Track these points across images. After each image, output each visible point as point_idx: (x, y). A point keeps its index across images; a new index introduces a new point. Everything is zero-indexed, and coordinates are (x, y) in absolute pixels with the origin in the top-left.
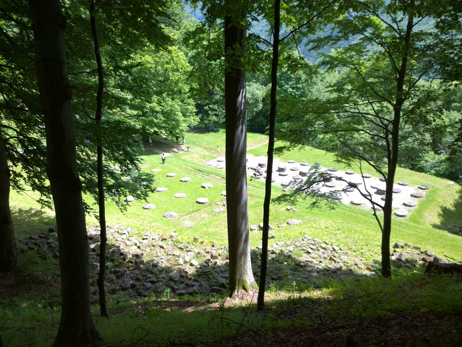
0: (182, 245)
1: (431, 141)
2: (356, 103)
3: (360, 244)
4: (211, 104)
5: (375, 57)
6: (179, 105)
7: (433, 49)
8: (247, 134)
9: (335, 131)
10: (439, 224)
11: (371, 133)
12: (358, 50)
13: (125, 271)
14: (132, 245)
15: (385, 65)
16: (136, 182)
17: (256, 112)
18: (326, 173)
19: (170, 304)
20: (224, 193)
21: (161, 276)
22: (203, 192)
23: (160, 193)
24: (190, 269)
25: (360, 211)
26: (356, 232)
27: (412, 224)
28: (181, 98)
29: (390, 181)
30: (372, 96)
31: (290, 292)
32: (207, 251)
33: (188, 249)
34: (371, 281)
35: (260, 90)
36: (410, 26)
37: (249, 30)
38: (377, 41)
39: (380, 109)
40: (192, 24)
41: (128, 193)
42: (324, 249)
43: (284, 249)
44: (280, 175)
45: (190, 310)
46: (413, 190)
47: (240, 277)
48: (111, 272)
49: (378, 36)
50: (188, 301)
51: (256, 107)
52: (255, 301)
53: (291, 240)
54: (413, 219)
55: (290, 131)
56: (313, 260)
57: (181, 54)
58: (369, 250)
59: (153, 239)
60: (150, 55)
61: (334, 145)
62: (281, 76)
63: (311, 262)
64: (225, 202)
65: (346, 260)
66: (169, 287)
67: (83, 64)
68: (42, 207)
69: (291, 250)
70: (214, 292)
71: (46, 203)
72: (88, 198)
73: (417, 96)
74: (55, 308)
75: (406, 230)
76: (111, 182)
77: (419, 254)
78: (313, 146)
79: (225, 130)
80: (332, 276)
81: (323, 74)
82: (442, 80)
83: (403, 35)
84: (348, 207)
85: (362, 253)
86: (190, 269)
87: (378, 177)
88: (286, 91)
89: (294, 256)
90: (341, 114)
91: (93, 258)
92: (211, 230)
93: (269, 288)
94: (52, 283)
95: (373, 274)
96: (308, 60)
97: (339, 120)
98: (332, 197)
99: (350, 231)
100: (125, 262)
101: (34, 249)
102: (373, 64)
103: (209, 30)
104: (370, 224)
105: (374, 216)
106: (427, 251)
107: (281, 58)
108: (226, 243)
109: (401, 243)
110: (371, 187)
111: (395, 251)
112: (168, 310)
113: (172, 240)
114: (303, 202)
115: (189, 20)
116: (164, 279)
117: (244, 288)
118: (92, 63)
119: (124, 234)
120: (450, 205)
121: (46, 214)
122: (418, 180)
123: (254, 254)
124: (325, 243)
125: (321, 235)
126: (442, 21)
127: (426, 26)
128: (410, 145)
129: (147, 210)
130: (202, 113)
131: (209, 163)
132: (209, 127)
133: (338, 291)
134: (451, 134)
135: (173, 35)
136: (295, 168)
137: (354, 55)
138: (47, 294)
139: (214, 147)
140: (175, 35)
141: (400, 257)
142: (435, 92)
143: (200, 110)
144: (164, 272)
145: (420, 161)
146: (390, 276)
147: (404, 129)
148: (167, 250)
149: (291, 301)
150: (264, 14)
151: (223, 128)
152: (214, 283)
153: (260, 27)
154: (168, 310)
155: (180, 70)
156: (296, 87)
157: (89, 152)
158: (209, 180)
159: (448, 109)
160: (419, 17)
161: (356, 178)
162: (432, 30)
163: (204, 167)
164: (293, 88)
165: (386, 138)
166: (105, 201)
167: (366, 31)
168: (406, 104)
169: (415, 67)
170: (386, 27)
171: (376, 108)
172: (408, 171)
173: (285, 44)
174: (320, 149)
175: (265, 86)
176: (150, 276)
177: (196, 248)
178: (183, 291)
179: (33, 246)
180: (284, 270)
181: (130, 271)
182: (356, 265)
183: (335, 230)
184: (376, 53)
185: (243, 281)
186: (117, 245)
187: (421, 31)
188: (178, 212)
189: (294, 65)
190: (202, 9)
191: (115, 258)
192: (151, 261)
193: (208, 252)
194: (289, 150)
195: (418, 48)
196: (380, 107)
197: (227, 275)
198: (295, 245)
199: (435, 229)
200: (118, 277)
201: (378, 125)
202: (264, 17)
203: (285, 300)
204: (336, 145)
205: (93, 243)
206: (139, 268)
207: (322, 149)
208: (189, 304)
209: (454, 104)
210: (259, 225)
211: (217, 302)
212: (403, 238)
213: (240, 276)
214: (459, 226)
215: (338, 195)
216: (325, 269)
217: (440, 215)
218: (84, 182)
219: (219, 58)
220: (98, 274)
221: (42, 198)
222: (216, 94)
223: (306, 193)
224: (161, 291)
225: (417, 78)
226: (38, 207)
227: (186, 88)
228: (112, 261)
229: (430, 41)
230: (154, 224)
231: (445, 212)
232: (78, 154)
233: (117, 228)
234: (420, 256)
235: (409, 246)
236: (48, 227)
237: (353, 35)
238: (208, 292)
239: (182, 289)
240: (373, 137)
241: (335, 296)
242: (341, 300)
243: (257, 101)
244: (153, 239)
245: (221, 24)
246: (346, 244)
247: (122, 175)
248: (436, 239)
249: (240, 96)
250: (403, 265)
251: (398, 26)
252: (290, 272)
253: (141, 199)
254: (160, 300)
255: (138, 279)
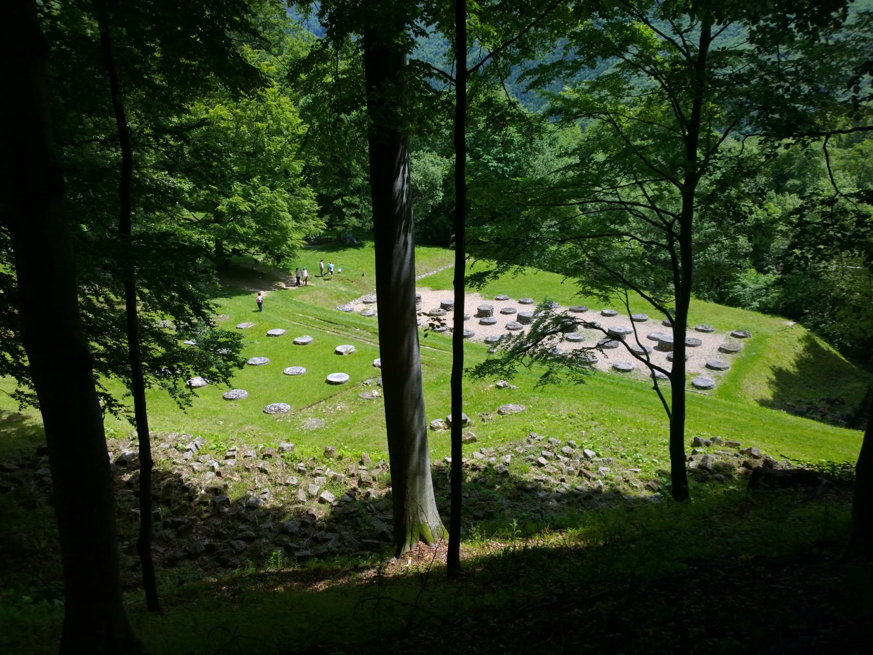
0: (302, 464)
1: (751, 250)
2: (613, 185)
3: (633, 442)
4: (346, 195)
5: (644, 98)
6: (284, 199)
7: (748, 82)
8: (417, 249)
9: (578, 238)
10: (771, 398)
11: (644, 239)
12: (615, 85)
13: (195, 521)
14: (205, 471)
15: (663, 112)
16: (206, 349)
17: (432, 206)
18: (566, 317)
19: (281, 577)
20: (377, 361)
21: (264, 526)
22: (339, 362)
23: (256, 368)
24: (319, 509)
25: (631, 382)
26: (624, 421)
27: (723, 401)
28: (288, 185)
29: (679, 325)
30: (641, 170)
31: (507, 539)
32: (352, 472)
33: (314, 472)
34: (654, 510)
35: (438, 165)
36: (706, 39)
37: (411, 53)
38: (648, 68)
39: (656, 193)
40: (304, 44)
41: (192, 372)
42: (569, 456)
44: (481, 323)
45: (321, 586)
46: (720, 340)
47: (413, 519)
48: (166, 526)
49: (649, 61)
50: (318, 570)
51: (432, 197)
52: (443, 559)
53: (508, 443)
54: (725, 393)
55: (498, 240)
57: (285, 100)
58: (649, 454)
59: (245, 457)
60: (226, 105)
61: (577, 264)
62: (476, 138)
63: (545, 482)
64: (380, 379)
65: (608, 474)
66: (280, 545)
67: (91, 125)
68: (21, 407)
69: (508, 461)
70: (368, 549)
71: (29, 399)
72: (113, 385)
73: (719, 168)
74: (56, 602)
75: (713, 413)
76: (159, 351)
77: (737, 456)
78: (541, 267)
79: (373, 244)
80: (583, 506)
81: (554, 132)
82: (762, 138)
83: (694, 57)
84: (609, 377)
85: (636, 460)
86: (319, 509)
87: (659, 319)
88: (486, 165)
89: (513, 473)
90: (589, 206)
91: (129, 500)
92: (356, 433)
93: (469, 536)
94: (50, 554)
95: (656, 497)
96: (525, 107)
97: (583, 217)
98: (578, 361)
99: (613, 420)
100: (192, 504)
101: (9, 489)
102: (641, 112)
103: (336, 54)
104: (649, 406)
105: (655, 391)
106: (751, 449)
107: (474, 104)
108: (384, 455)
109: (705, 437)
110: (649, 337)
111: (694, 453)
112: (280, 589)
113: (282, 457)
114: (527, 373)
115: (299, 37)
116: (271, 531)
117: (423, 538)
118: (111, 122)
119: (188, 450)
120: (788, 363)
121: (30, 421)
122: (731, 320)
123: (438, 473)
124: (569, 444)
125: (561, 431)
126: (761, 30)
127: (736, 38)
128: (715, 258)
129: (232, 403)
130: (330, 212)
131: (348, 307)
132: (345, 238)
133: (594, 532)
134: (785, 234)
135: (268, 66)
136: (510, 309)
137: (607, 95)
138: (41, 575)
139: (356, 275)
140: (272, 65)
141: (704, 463)
142: (752, 160)
143: (326, 206)
144: (270, 518)
145: (732, 287)
146: (687, 497)
147: (701, 229)
148: (274, 475)
149: (509, 557)
150: (437, 22)
151: (371, 240)
152: (366, 533)
153: (431, 47)
154: (280, 589)
155: (285, 132)
156: (505, 157)
157: (112, 296)
158: (348, 340)
159: (780, 190)
160: (718, 24)
161: (620, 323)
162: (740, 48)
163: (338, 314)
164: (499, 160)
165: (670, 248)
166: (146, 390)
167: (627, 51)
168: (704, 183)
169: (717, 116)
170: (663, 43)
171: (650, 194)
172: (712, 305)
173: (480, 79)
174: (552, 271)
175: (448, 157)
176: (242, 527)
177: (329, 469)
178: (308, 552)
179: (7, 484)
180: (495, 501)
181: (202, 520)
182: (627, 481)
183: (587, 420)
184: (647, 91)
185: (419, 524)
186: (176, 471)
187: (724, 48)
188: (291, 404)
189: (500, 117)
190: (321, 15)
191: (173, 497)
192: (243, 498)
193: (353, 475)
194: (495, 277)
195: (719, 79)
196: (657, 190)
197: (390, 516)
198: (516, 453)
199: (764, 409)
200: (179, 535)
201: (654, 224)
202: (438, 28)
203: (499, 556)
204: (582, 264)
205: (128, 471)
206: (219, 514)
207: (558, 272)
208: (319, 575)
209: (790, 182)
210: (447, 419)
211: (373, 567)
212: (708, 427)
213: (414, 517)
214: (807, 401)
215: (589, 356)
216: (572, 493)
217: (771, 382)
218: (103, 355)
219: (356, 107)
220: (139, 530)
221: (20, 390)
222: (356, 176)
223: (531, 356)
224: (266, 554)
225: (720, 136)
226: (13, 406)
227: (298, 166)
228: (168, 503)
229: (742, 67)
230: (247, 428)
231: (781, 377)
232: (90, 300)
233: (174, 440)
234: (739, 459)
235: (719, 442)
236: (37, 445)
237: (604, 58)
238: (356, 551)
239: (306, 548)
240: (648, 245)
241: (588, 541)
242: (599, 548)
243: (433, 187)
244: (245, 457)
245: (357, 42)
246: (607, 445)
247: (180, 337)
248: (767, 426)
249: (400, 178)
250: (710, 476)
251: (684, 41)
252: (506, 502)
253: (218, 382)
254: (262, 571)
255: (218, 536)
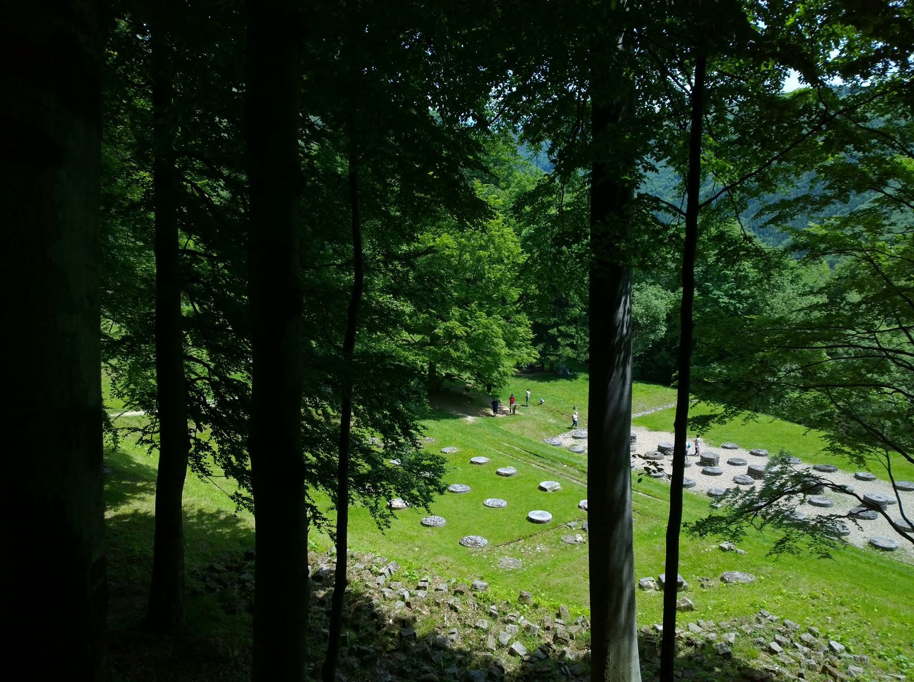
3: (895, 640)
42: (808, 645)
43: (712, 636)
44: (704, 472)
56: (783, 670)
85: (899, 663)
114: (759, 537)
124: (811, 631)
198: (741, 631)
